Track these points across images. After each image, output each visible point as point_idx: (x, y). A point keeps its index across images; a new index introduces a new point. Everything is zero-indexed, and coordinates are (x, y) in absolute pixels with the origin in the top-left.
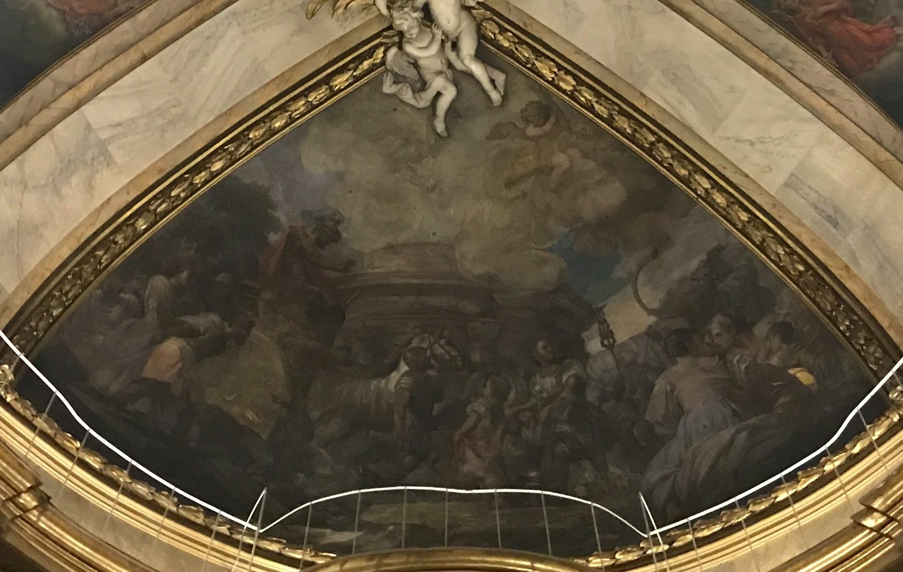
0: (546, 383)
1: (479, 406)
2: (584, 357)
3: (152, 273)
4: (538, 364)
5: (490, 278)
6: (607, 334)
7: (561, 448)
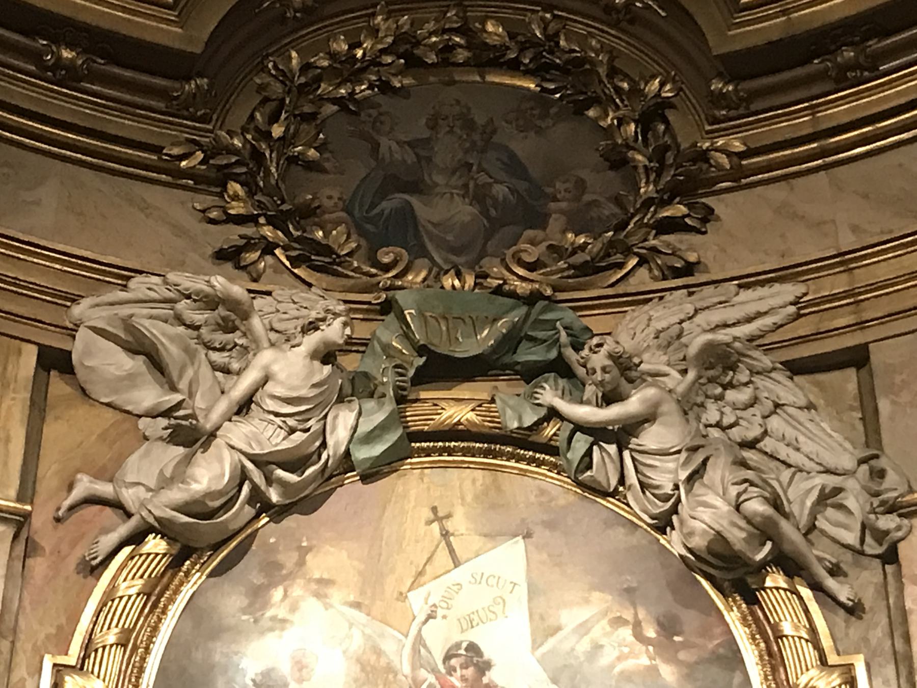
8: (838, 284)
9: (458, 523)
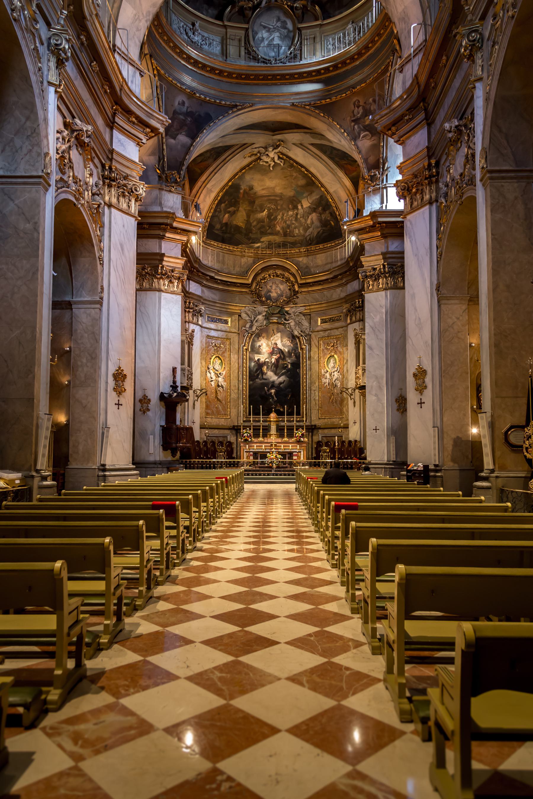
0: (291, 213)
1: (279, 217)
2: (298, 209)
3: (221, 204)
4: (289, 209)
5: (281, 193)
6: (302, 206)
7: (293, 226)
8: (309, 308)
9: (275, 331)
